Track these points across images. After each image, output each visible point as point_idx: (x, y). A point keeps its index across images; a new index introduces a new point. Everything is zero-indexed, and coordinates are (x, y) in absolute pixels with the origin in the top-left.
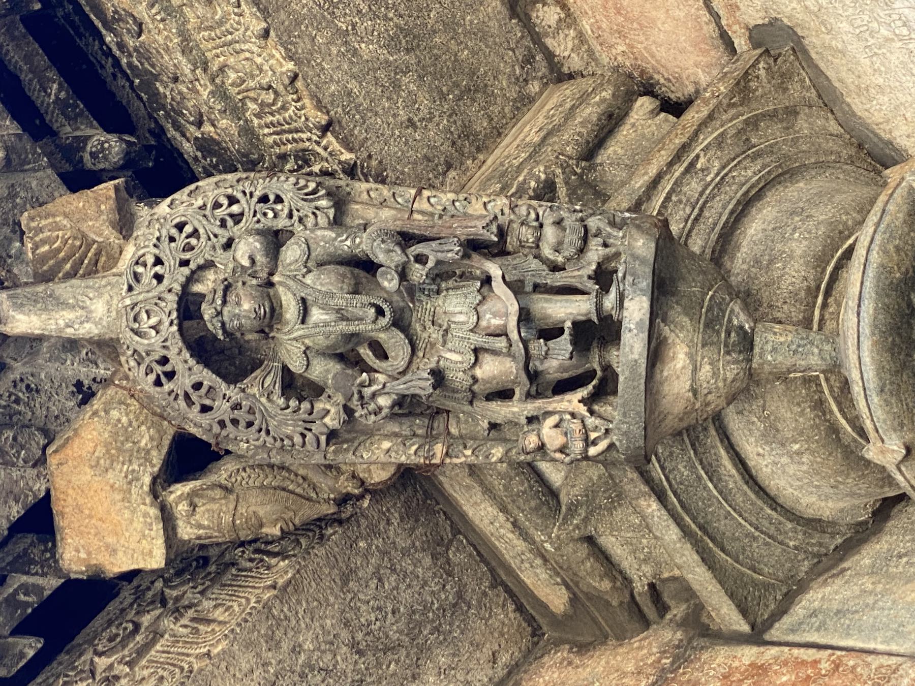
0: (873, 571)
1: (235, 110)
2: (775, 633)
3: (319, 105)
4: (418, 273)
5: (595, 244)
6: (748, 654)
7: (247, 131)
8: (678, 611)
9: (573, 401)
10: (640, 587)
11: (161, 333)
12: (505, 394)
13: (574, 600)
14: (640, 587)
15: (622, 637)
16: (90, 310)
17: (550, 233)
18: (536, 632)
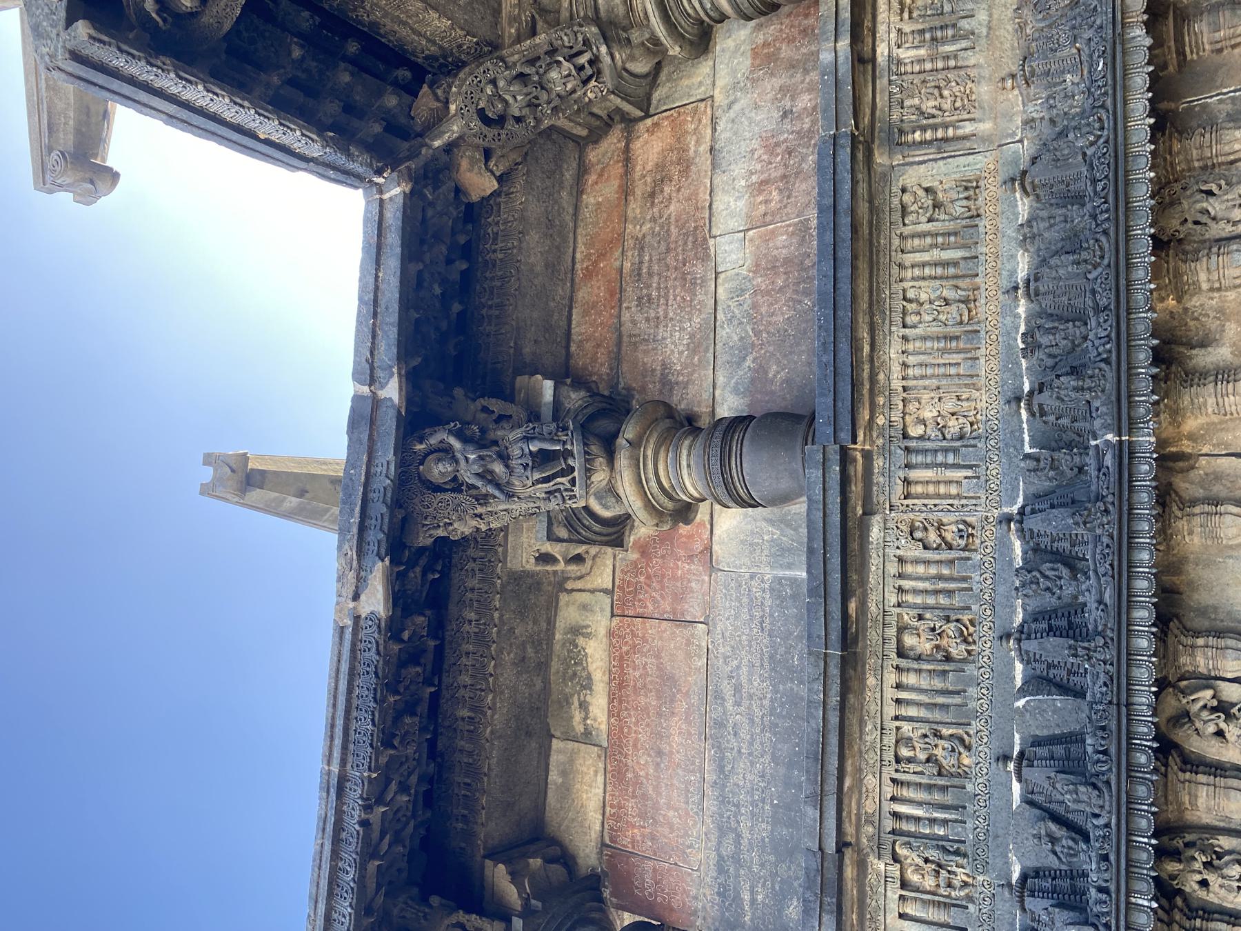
0: (668, 80)
1: (434, 43)
2: (652, 111)
3: (462, 29)
4: (541, 71)
5: (579, 35)
6: (649, 122)
7: (441, 47)
8: (617, 118)
9: (593, 83)
10: (605, 117)
11: (476, 124)
12: (574, 91)
13: (590, 131)
14: (605, 117)
15: (606, 134)
16: (454, 129)
17: (565, 38)
18: (579, 144)
